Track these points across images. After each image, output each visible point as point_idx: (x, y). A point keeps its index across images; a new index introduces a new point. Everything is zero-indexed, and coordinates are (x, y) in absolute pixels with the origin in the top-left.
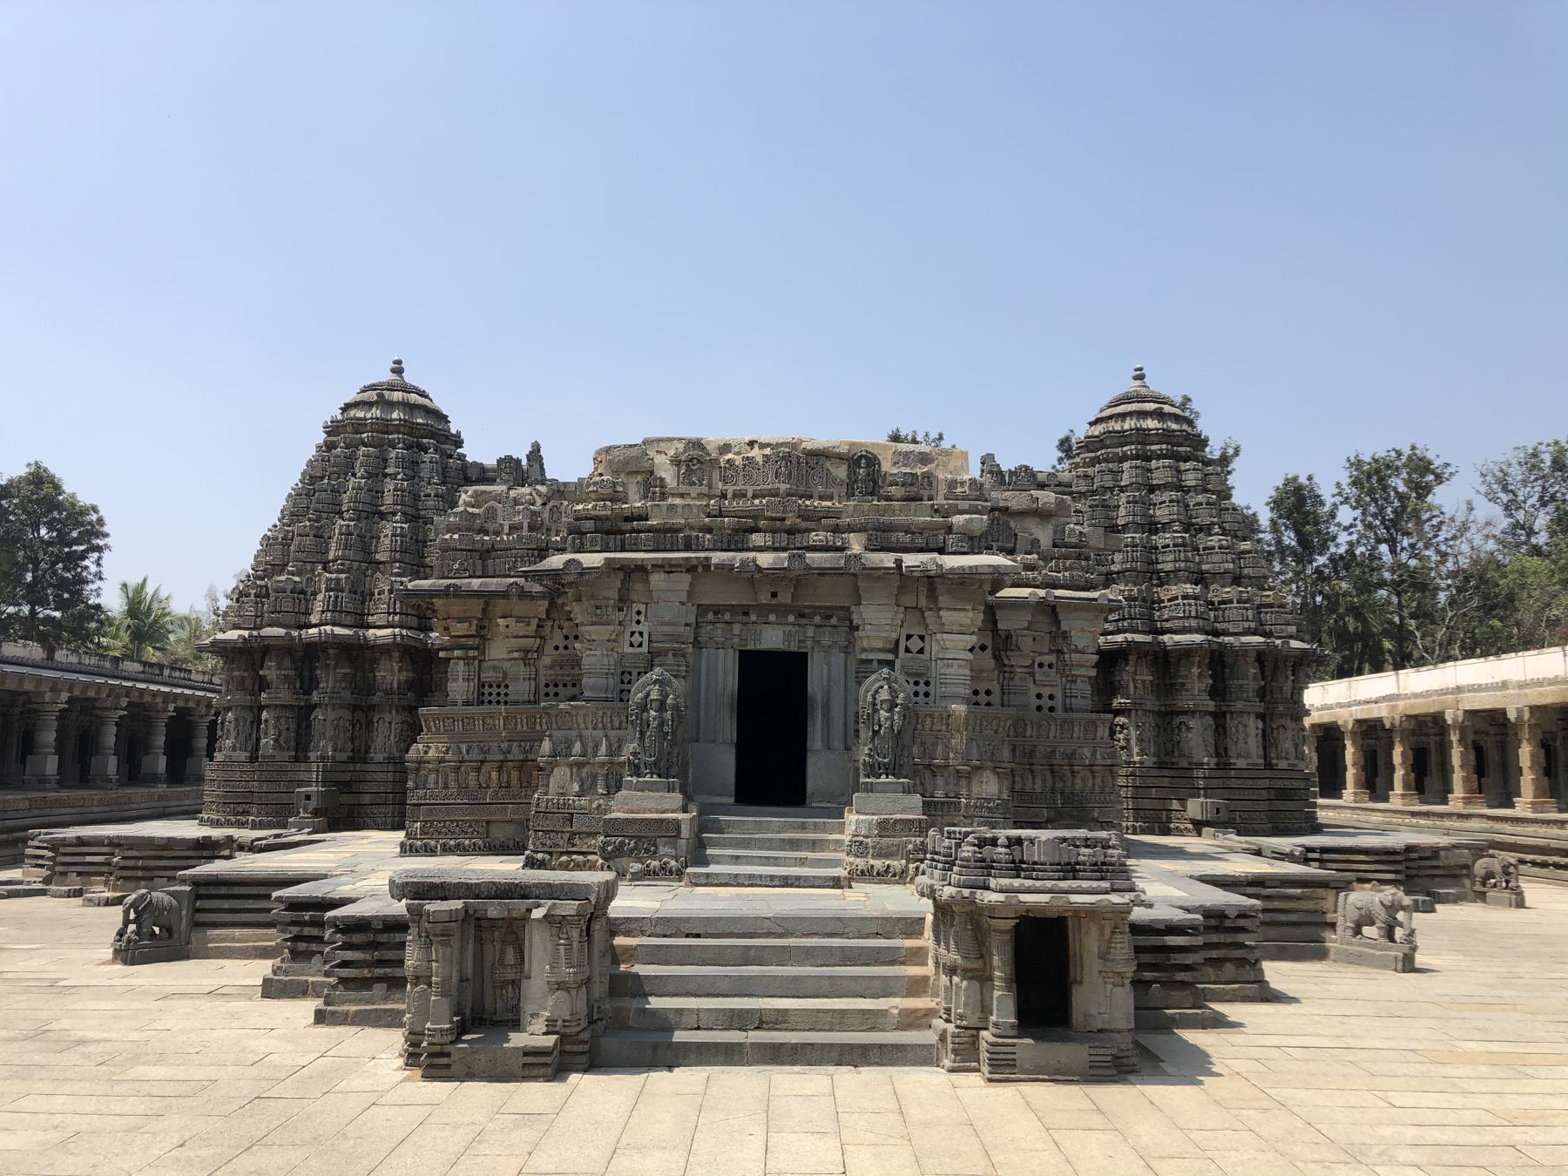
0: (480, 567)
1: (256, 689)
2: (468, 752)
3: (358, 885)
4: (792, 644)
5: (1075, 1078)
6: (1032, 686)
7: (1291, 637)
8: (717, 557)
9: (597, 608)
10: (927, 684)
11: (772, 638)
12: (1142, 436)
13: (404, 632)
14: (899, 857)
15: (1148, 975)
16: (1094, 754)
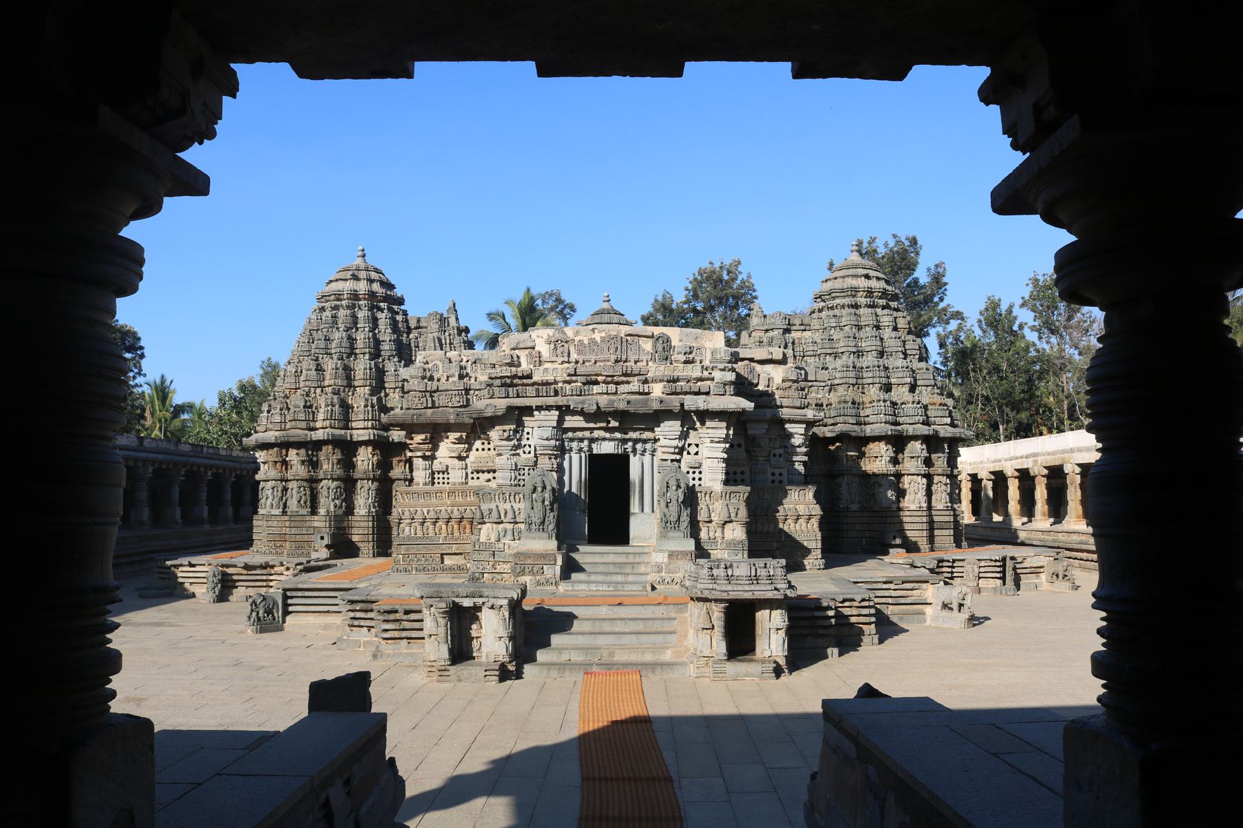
0: (430, 402)
1: (284, 469)
2: (428, 513)
3: (379, 591)
4: (620, 451)
5: (755, 679)
6: (769, 468)
7: (946, 424)
8: (573, 402)
9: (504, 431)
10: (700, 473)
11: (607, 448)
12: (854, 291)
13: (375, 432)
14: (680, 574)
15: (805, 632)
16: (805, 509)
